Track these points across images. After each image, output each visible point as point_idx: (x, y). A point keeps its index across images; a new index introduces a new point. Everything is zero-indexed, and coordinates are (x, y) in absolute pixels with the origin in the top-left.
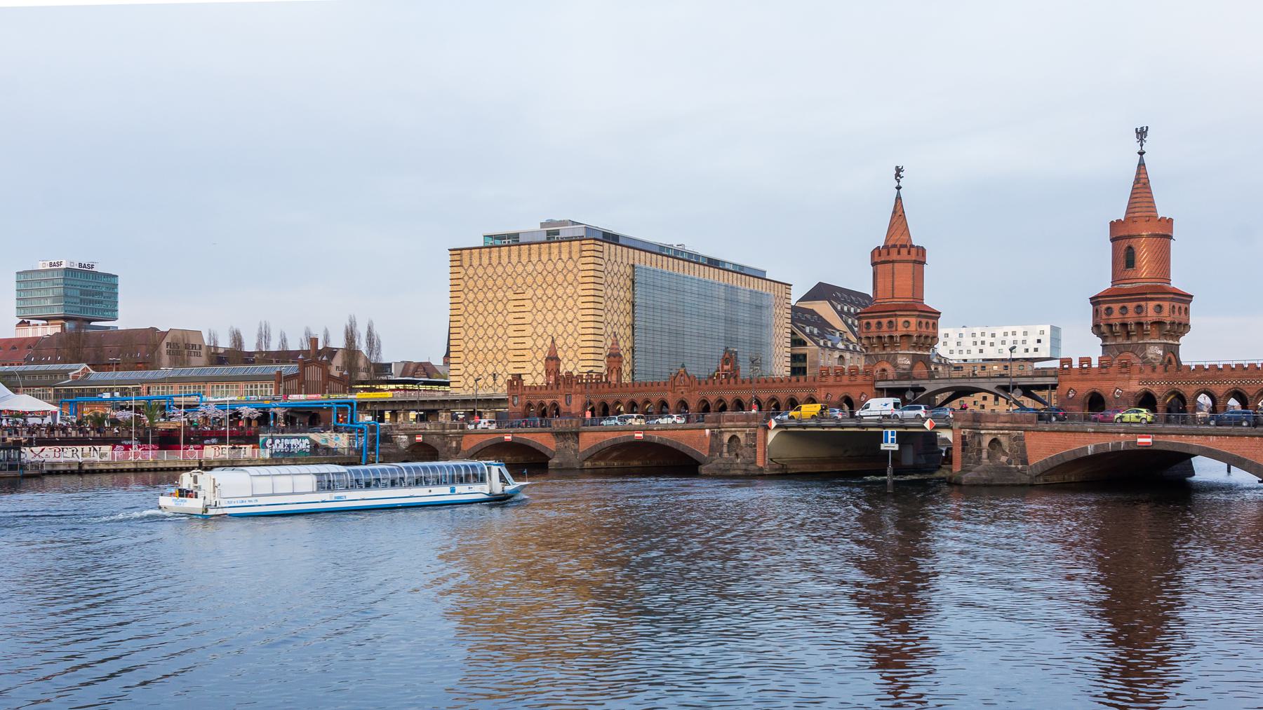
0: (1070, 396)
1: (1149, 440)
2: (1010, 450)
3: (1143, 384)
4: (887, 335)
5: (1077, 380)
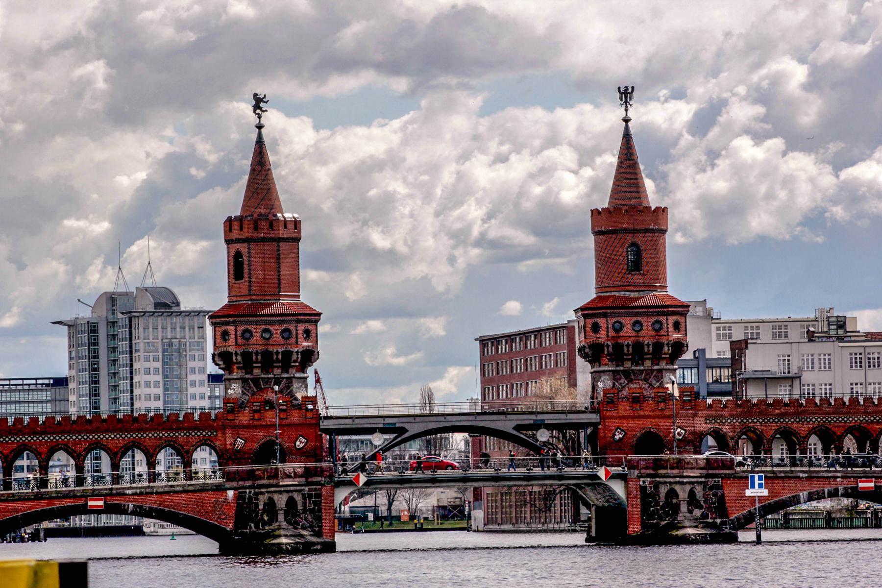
0: (617, 437)
1: (872, 485)
2: (705, 502)
3: (711, 422)
4: (280, 350)
5: (625, 417)
